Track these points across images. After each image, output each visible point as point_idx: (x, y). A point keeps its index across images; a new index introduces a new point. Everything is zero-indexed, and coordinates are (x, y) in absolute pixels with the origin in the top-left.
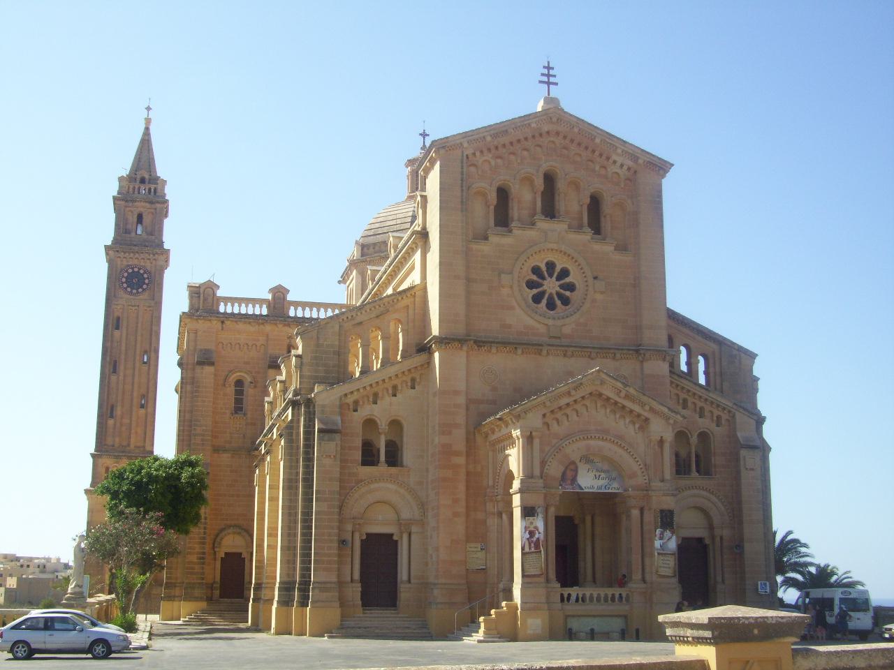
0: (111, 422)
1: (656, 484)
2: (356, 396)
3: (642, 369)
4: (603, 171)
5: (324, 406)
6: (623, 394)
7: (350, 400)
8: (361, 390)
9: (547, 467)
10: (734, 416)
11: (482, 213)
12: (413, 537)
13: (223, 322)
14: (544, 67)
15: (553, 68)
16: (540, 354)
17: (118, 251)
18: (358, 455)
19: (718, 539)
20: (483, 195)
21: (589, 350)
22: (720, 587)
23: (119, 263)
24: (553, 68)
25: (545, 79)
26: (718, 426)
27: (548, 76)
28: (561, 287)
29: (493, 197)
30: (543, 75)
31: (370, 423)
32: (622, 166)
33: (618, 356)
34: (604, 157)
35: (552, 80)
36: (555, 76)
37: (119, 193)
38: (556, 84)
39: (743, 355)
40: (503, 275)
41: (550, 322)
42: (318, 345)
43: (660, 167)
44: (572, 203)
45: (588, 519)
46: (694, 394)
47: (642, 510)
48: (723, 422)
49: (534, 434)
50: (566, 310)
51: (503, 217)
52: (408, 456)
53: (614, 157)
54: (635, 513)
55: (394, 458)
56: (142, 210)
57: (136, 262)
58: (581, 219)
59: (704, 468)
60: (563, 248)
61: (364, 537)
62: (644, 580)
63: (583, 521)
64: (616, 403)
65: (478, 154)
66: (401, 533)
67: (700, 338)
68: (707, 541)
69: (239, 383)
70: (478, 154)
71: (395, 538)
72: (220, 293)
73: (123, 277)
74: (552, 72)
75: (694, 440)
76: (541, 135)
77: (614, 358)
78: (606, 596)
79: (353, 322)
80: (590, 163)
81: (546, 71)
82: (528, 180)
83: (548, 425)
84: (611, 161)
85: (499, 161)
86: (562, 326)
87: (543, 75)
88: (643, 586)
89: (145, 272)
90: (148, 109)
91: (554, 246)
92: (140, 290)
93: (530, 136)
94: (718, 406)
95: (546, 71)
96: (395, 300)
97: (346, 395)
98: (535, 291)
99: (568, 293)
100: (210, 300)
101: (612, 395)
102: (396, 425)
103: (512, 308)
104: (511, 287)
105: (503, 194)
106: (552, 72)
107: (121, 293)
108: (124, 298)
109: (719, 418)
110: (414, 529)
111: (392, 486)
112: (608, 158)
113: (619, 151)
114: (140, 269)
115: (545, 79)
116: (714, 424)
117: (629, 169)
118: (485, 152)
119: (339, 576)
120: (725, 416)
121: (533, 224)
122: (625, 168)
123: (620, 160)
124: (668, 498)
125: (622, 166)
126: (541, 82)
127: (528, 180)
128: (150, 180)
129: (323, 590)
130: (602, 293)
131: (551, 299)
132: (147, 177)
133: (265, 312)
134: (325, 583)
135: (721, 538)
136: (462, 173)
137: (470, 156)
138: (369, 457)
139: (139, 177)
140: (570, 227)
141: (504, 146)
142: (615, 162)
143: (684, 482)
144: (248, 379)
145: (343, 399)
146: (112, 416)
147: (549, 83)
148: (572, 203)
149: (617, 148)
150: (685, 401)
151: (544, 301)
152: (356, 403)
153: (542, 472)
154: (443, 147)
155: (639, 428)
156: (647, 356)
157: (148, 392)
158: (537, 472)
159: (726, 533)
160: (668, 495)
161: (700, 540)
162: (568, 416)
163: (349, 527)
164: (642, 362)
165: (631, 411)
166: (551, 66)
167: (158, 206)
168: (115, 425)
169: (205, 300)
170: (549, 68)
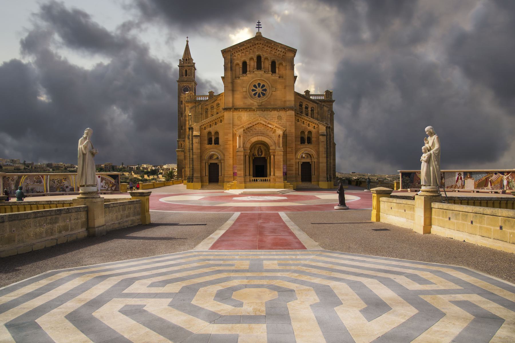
0: (182, 131)
2: (205, 126)
3: (286, 114)
4: (275, 54)
5: (195, 129)
6: (267, 123)
7: (203, 127)
8: (206, 124)
9: (245, 144)
10: (319, 126)
12: (222, 164)
13: (195, 103)
14: (258, 23)
15: (260, 23)
16: (254, 111)
17: (180, 82)
18: (206, 142)
19: (313, 162)
20: (238, 64)
21: (269, 109)
22: (313, 176)
23: (181, 85)
24: (260, 23)
25: (258, 26)
26: (314, 129)
27: (259, 25)
28: (262, 90)
29: (241, 65)
30: (257, 25)
31: (209, 133)
32: (281, 51)
33: (278, 110)
34: (275, 49)
35: (260, 26)
36: (261, 25)
37: (179, 64)
38: (261, 27)
39: (324, 107)
40: (244, 88)
41: (258, 101)
42: (195, 112)
44: (267, 65)
45: (269, 158)
46: (306, 120)
47: (274, 156)
48: (316, 128)
49: (241, 135)
50: (264, 97)
51: (245, 71)
53: (279, 49)
54: (272, 157)
55: (217, 142)
57: (186, 85)
58: (269, 69)
59: (309, 141)
60: (262, 79)
61: (209, 164)
62: (274, 175)
63: (267, 158)
64: (266, 125)
65: (236, 52)
67: (311, 102)
68: (310, 163)
70: (236, 52)
71: (218, 164)
73: (182, 89)
74: (260, 24)
75: (306, 133)
76: (255, 44)
77: (277, 111)
78: (255, 180)
79: (205, 105)
80: (271, 51)
81: (258, 24)
82: (252, 59)
83: (246, 133)
84: (278, 50)
85: (243, 54)
86: (262, 102)
87: (257, 25)
88: (274, 177)
90: (187, 37)
91: (260, 79)
93: (251, 45)
94: (314, 123)
95: (258, 24)
96: (217, 98)
97: (202, 126)
98: (254, 92)
99: (264, 92)
100: (192, 97)
101: (264, 123)
102: (217, 133)
104: (246, 92)
105: (245, 64)
106: (260, 24)
107: (182, 94)
109: (314, 126)
110: (222, 161)
111: (216, 150)
112: (277, 50)
114: (187, 86)
115: (258, 26)
116: (313, 129)
117: (283, 52)
118: (238, 51)
119: (201, 175)
120: (316, 126)
121: (254, 72)
122: (282, 52)
123: (280, 50)
124: (281, 152)
125: (281, 51)
126: (256, 27)
127: (252, 59)
128: (188, 59)
129: (196, 178)
130: (274, 91)
131: (259, 94)
132: (188, 59)
133: (207, 98)
134: (197, 176)
135: (314, 162)
136: (231, 59)
137: (233, 53)
138: (210, 142)
139: (185, 59)
140: (264, 72)
141: (244, 49)
142: (279, 50)
145: (201, 126)
146: (182, 129)
147: (259, 27)
148: (267, 65)
149: (279, 46)
150: (303, 122)
151: (257, 95)
152: (205, 127)
153: (243, 146)
154: (225, 52)
155: (273, 132)
156: (287, 110)
158: (242, 146)
159: (316, 160)
160: (280, 151)
161: (309, 162)
163: (204, 162)
164: (286, 111)
165: (270, 128)
166: (260, 22)
167: (191, 67)
168: (183, 131)
169: (190, 97)
170: (259, 23)
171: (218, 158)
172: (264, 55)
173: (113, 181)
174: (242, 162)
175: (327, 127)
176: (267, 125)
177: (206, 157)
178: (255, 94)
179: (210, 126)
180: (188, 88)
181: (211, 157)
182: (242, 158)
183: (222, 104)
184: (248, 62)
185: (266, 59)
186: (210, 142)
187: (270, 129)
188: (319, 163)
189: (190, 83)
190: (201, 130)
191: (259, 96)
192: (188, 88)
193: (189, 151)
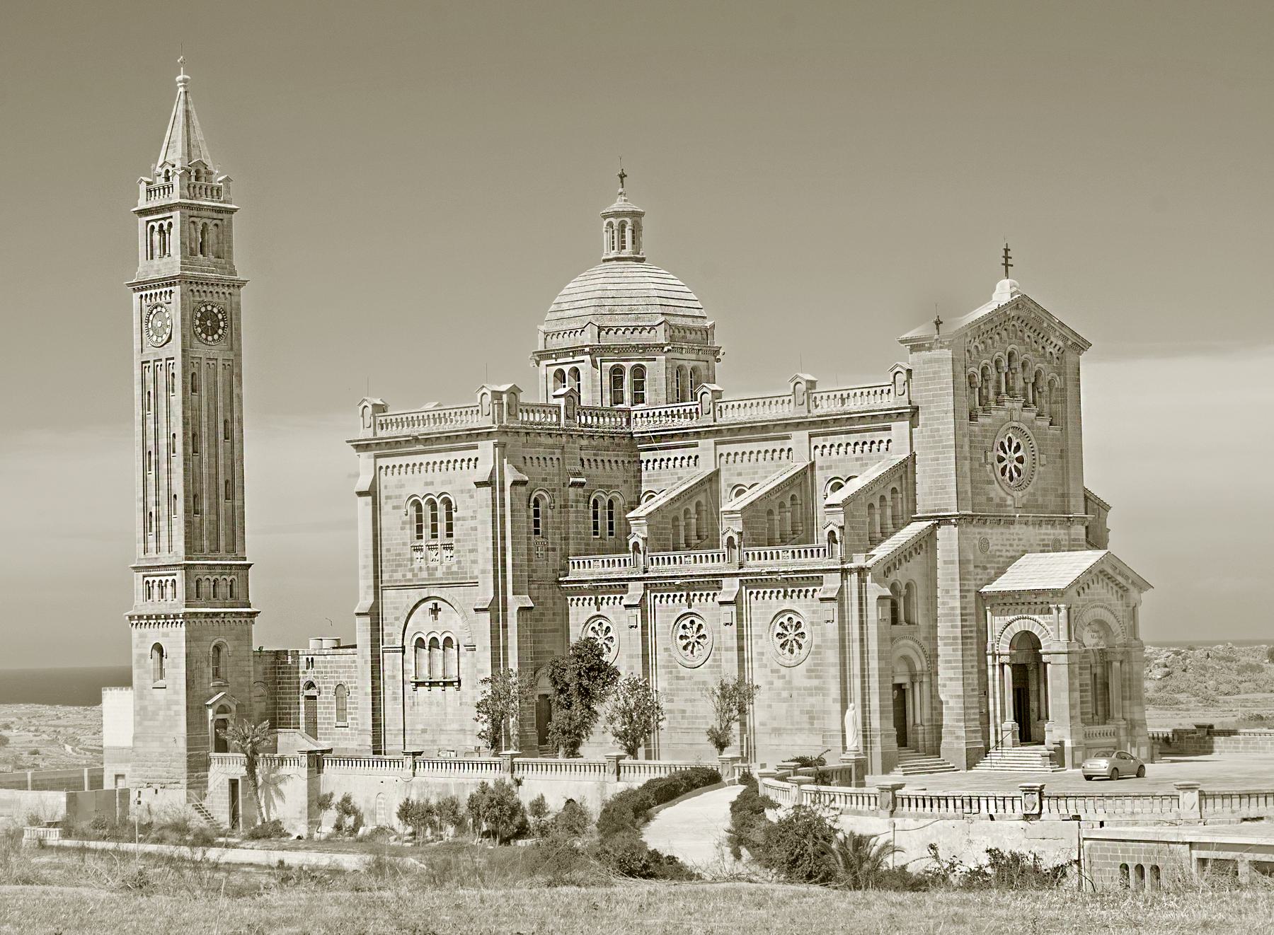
34: (1045, 339)
43: (1080, 346)
47: (1121, 662)
56: (208, 221)
66: (913, 684)
72: (523, 398)
79: (871, 492)
84: (1049, 342)
89: (219, 312)
91: (1015, 424)
92: (216, 337)
101: (1110, 571)
103: (991, 482)
107: (196, 341)
108: (200, 351)
110: (925, 679)
111: (911, 643)
113: (1057, 334)
114: (213, 307)
122: (1057, 347)
132: (203, 170)
147: (1006, 265)
157: (233, 478)
162: (1083, 589)
176: (1115, 575)
180: (220, 316)
183: (904, 493)
186: (895, 621)
187: (1115, 588)
189: (226, 290)
192: (212, 311)
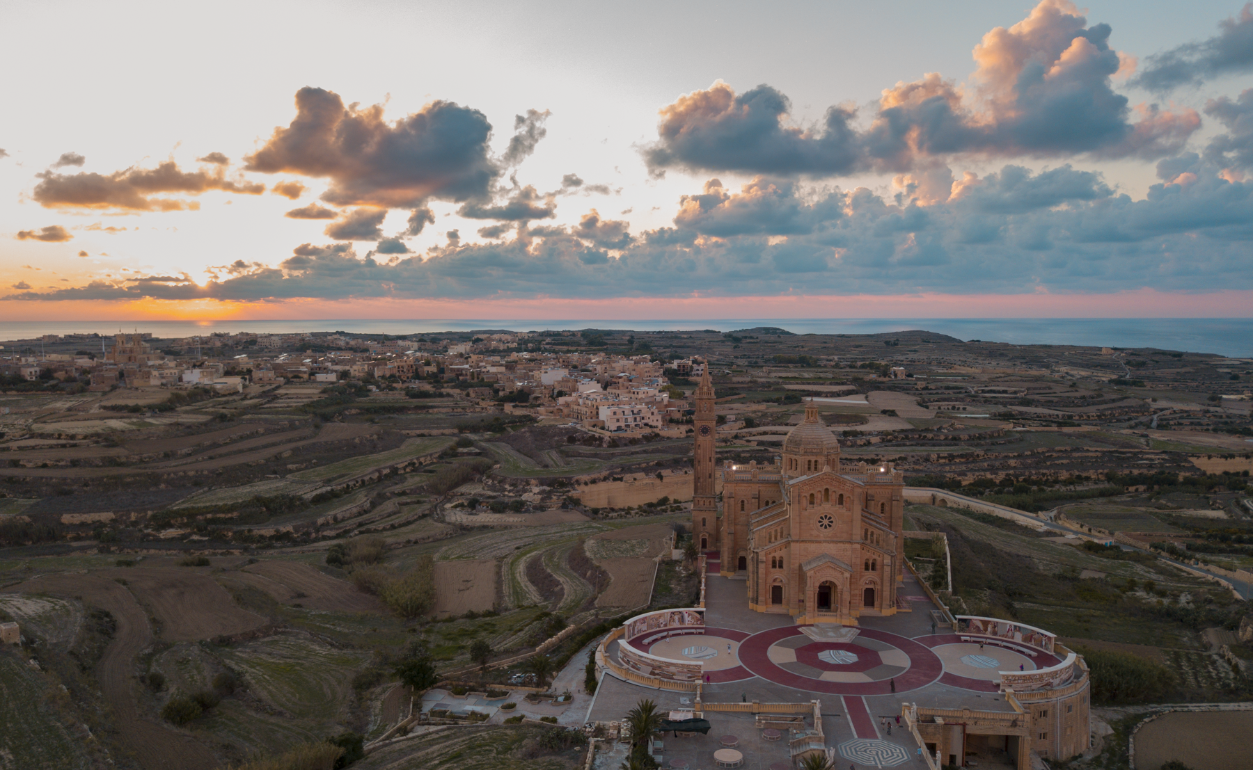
1: (845, 588)
11: (805, 502)
18: (771, 566)
31: (774, 557)
44: (834, 497)
52: (785, 565)
55: (781, 566)
59: (873, 569)
69: (743, 502)
138: (774, 566)
143: (867, 573)
144: (746, 502)
171: (781, 581)
172: (831, 489)
173: (698, 616)
174: (812, 600)
175: (892, 556)
177: (770, 580)
178: (821, 526)
179: (775, 551)
181: (775, 580)
182: (812, 596)
184: (815, 495)
185: (835, 492)
188: (882, 590)
190: (766, 554)
191: (826, 527)
193: (753, 574)
